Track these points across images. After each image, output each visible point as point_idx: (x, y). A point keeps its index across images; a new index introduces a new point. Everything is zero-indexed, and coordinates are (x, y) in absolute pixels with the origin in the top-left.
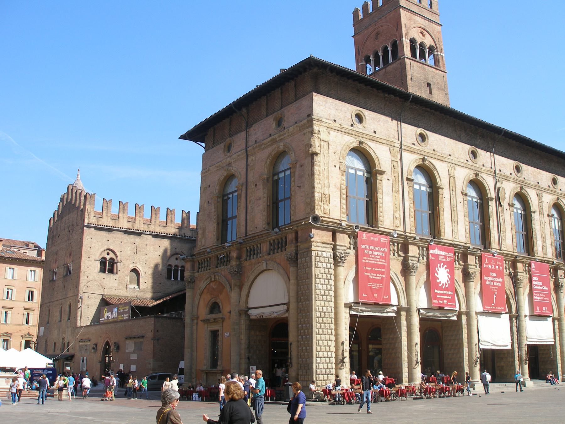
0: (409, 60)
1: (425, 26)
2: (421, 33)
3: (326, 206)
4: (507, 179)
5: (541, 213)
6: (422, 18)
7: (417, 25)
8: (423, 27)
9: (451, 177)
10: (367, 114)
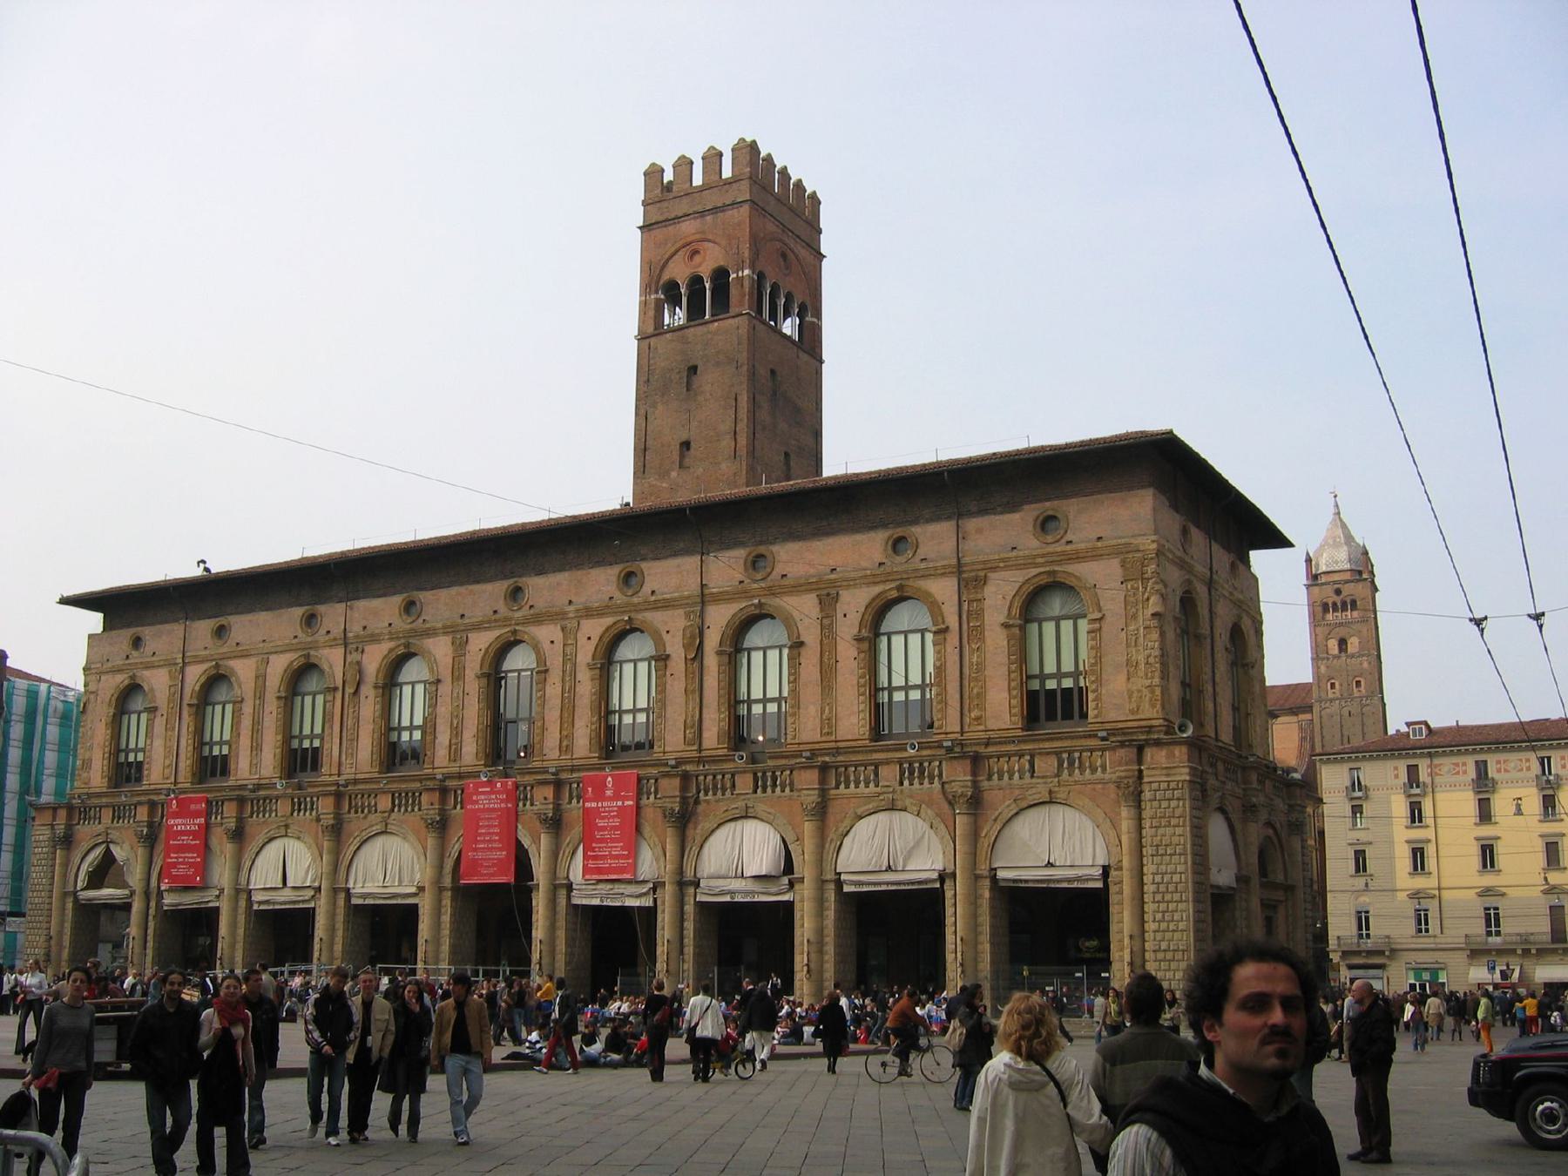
0: (648, 340)
1: (703, 232)
2: (696, 252)
3: (85, 775)
4: (374, 639)
5: (458, 674)
6: (694, 218)
7: (681, 243)
8: (698, 236)
9: (261, 678)
10: (146, 632)
